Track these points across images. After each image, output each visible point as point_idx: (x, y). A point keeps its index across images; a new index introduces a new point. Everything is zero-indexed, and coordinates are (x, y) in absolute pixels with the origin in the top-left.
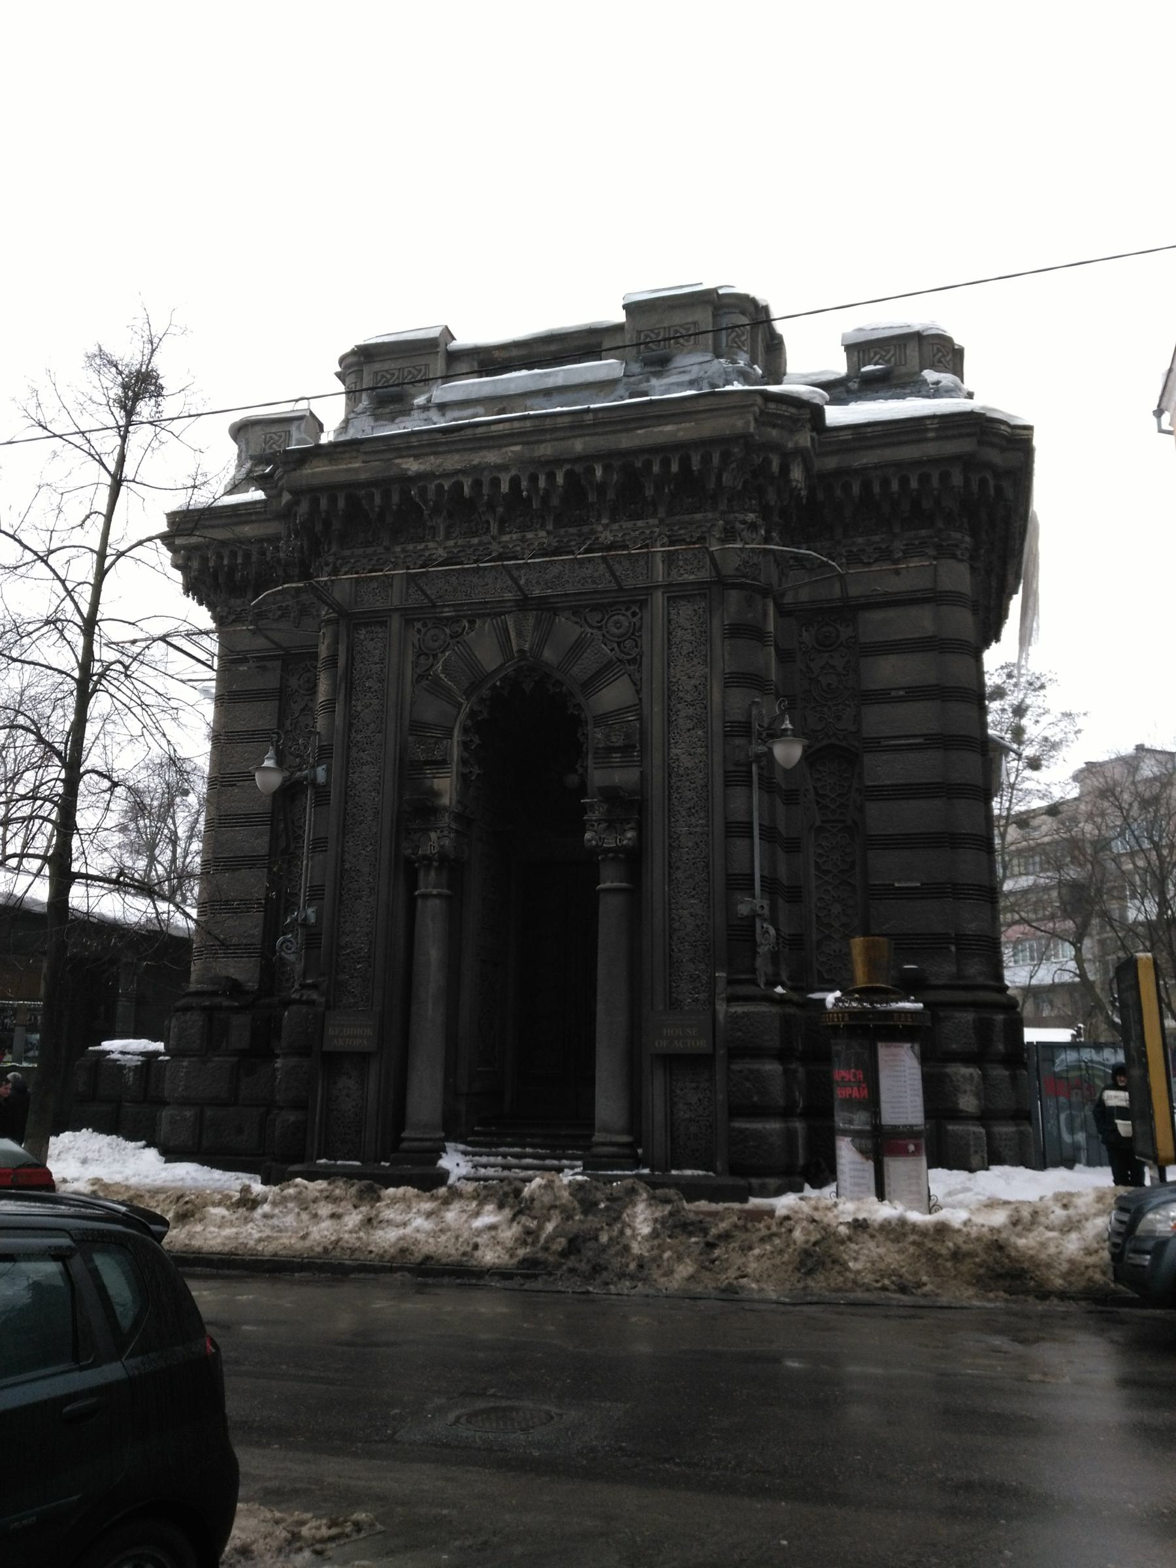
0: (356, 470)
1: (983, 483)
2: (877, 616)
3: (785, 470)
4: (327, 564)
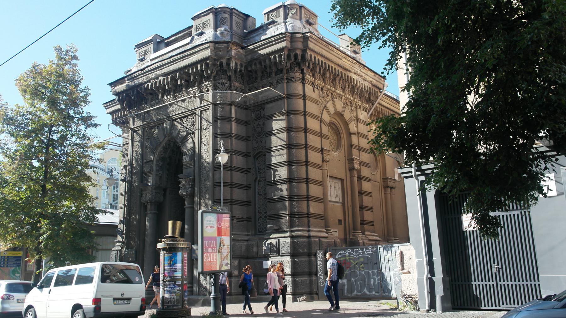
1: (296, 56)
3: (228, 64)
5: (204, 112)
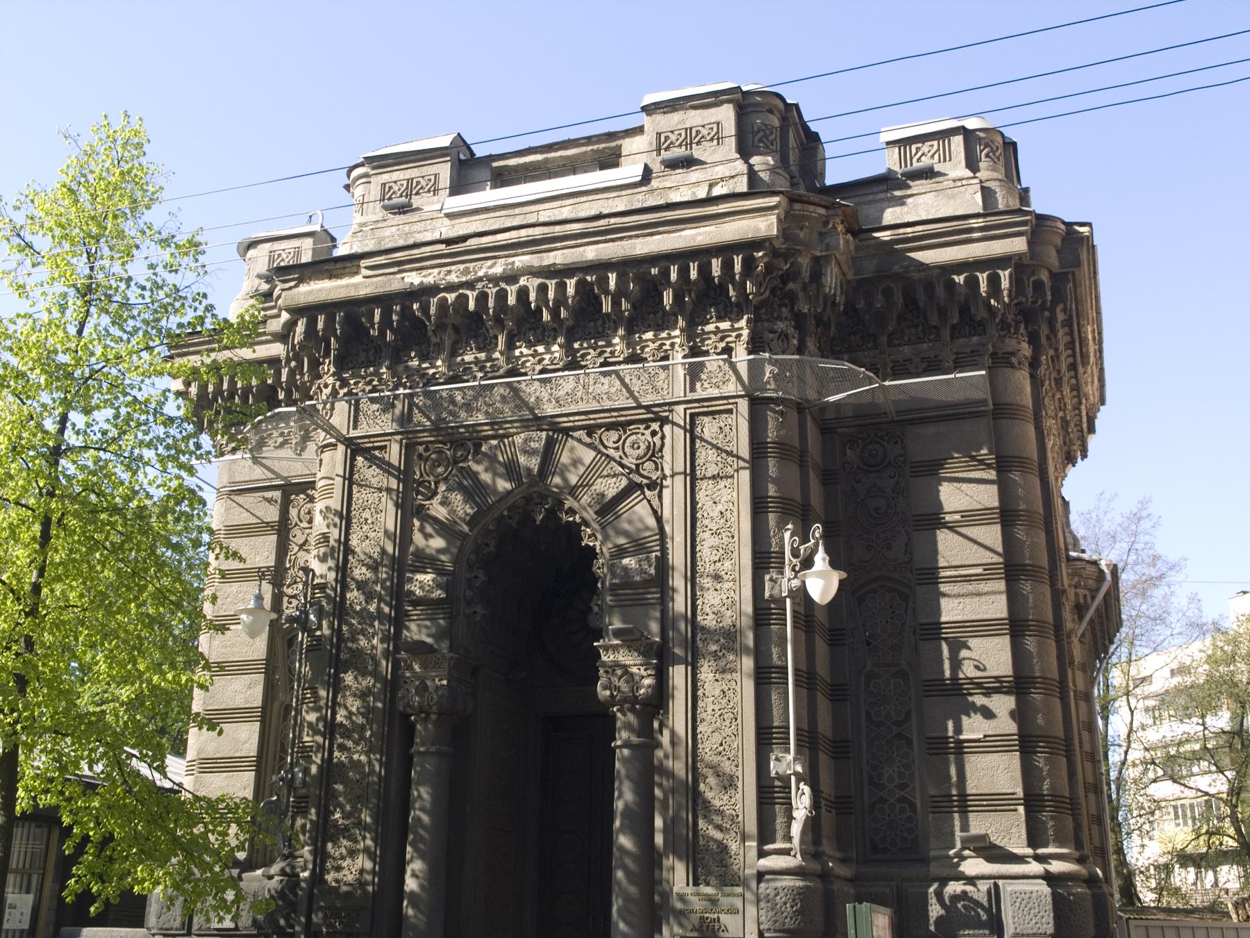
0: (356, 286)
1: (1038, 285)
2: (930, 430)
3: (817, 276)
4: (326, 386)
5: (706, 419)
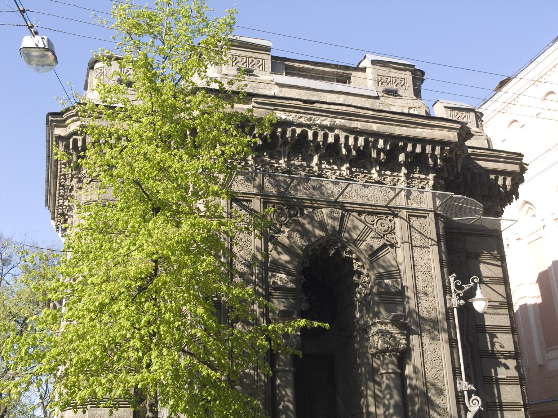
5: (414, 219)
